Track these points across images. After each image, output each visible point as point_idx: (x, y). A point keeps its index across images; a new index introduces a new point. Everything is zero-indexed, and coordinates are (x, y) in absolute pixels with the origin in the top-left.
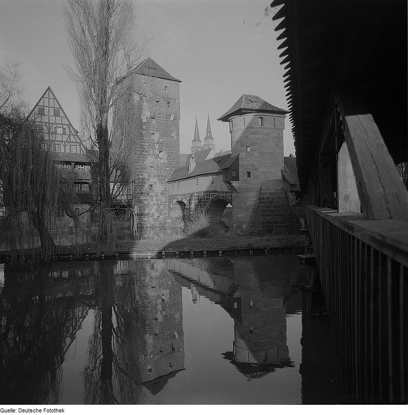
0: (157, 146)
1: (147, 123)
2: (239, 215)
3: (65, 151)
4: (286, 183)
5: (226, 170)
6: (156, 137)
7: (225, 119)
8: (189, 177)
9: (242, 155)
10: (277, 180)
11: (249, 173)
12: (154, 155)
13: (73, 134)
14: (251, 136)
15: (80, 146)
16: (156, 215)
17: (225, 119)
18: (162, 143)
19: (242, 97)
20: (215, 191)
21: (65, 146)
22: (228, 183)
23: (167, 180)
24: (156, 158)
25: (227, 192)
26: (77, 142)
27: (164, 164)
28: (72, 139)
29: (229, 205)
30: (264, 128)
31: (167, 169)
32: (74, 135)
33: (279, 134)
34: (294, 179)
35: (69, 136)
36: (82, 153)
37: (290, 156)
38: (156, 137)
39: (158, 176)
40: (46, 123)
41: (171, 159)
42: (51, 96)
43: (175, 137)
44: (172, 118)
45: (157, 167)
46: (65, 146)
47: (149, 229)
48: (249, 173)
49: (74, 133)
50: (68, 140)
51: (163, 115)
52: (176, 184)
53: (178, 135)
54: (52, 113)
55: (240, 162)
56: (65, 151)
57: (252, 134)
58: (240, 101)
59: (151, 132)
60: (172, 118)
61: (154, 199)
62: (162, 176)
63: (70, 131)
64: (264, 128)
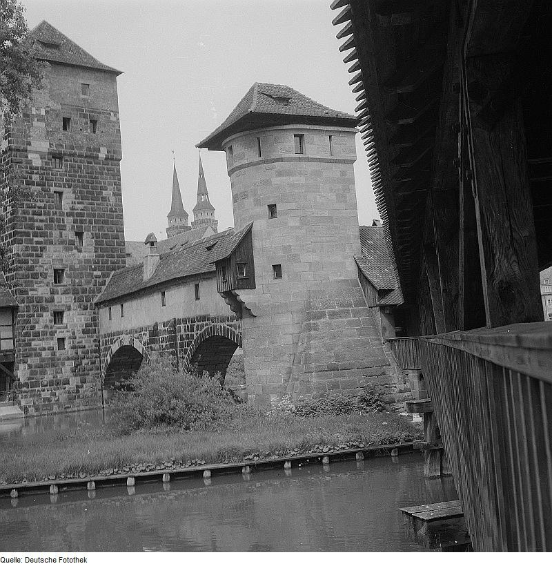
0: (69, 221)
1: (42, 168)
2: (259, 373)
4: (369, 289)
5: (223, 265)
6: (68, 197)
7: (214, 143)
8: (144, 289)
9: (261, 226)
10: (345, 281)
11: (277, 269)
12: (62, 243)
14: (277, 181)
16: (74, 382)
17: (214, 143)
18: (80, 215)
19: (252, 90)
20: (204, 318)
22: (230, 296)
23: (96, 300)
24: (67, 249)
25: (232, 319)
27: (88, 261)
29: (238, 351)
30: (309, 160)
31: (95, 273)
33: (343, 173)
34: (386, 276)
37: (374, 224)
38: (68, 197)
39: (75, 292)
41: (106, 250)
43: (112, 199)
44: (102, 154)
45: (72, 268)
47: (56, 419)
48: (277, 269)
51: (82, 148)
52: (116, 309)
53: (118, 194)
55: (256, 243)
57: (280, 174)
58: (248, 98)
59: (53, 189)
60: (102, 154)
61: (67, 344)
62: (84, 291)
64: (309, 160)
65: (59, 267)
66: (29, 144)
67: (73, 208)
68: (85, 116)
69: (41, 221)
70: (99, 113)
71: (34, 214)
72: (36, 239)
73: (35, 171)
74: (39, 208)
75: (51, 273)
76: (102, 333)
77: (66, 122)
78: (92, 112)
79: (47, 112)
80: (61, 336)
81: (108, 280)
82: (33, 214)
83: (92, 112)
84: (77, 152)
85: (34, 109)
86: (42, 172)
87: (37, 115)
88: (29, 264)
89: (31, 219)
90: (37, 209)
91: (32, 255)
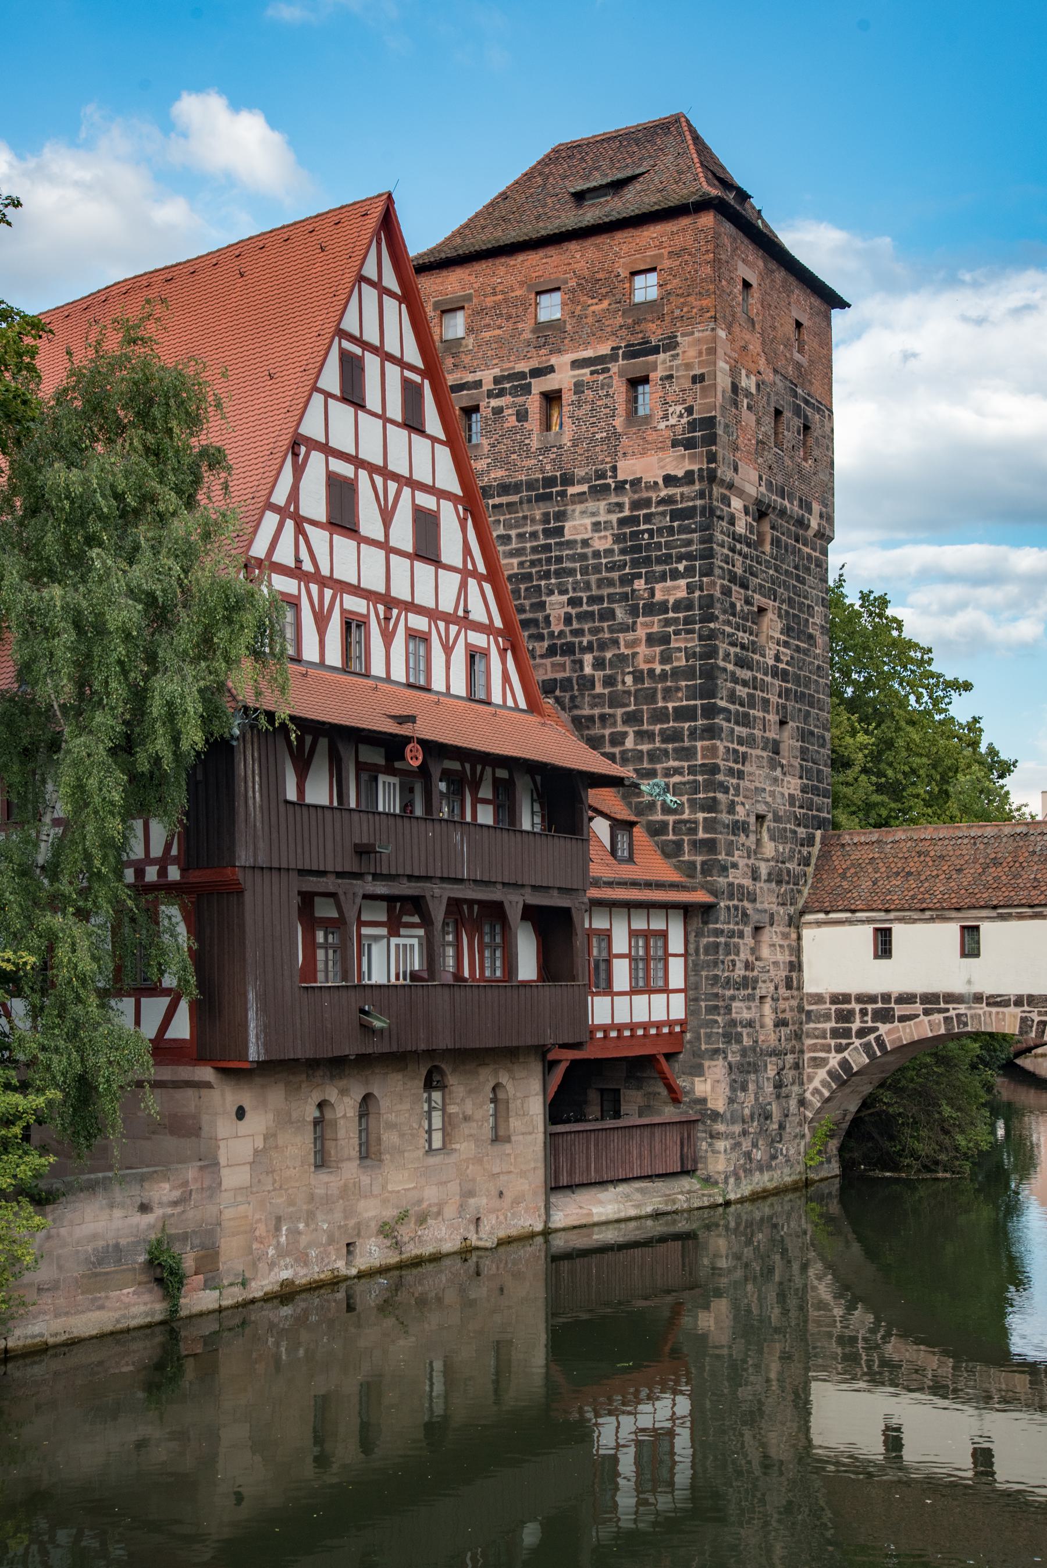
3: (448, 687)
13: (475, 574)
15: (502, 652)
18: (784, 676)
21: (448, 650)
26: (486, 629)
28: (478, 614)
32: (480, 578)
35: (466, 573)
36: (510, 703)
40: (372, 469)
42: (390, 281)
45: (777, 819)
46: (448, 650)
49: (482, 569)
50: (461, 613)
54: (395, 411)
56: (448, 687)
63: (467, 551)
65: (761, 809)
66: (736, 470)
67: (777, 658)
68: (797, 411)
69: (745, 683)
70: (813, 406)
71: (741, 663)
72: (737, 728)
73: (738, 546)
74: (743, 647)
75: (752, 820)
76: (809, 988)
77: (778, 413)
78: (807, 402)
79: (758, 386)
80: (764, 993)
81: (816, 850)
82: (736, 664)
83: (807, 402)
84: (788, 505)
85: (743, 372)
86: (745, 549)
87: (748, 394)
88: (731, 797)
89: (735, 680)
90: (738, 650)
91: (731, 772)
